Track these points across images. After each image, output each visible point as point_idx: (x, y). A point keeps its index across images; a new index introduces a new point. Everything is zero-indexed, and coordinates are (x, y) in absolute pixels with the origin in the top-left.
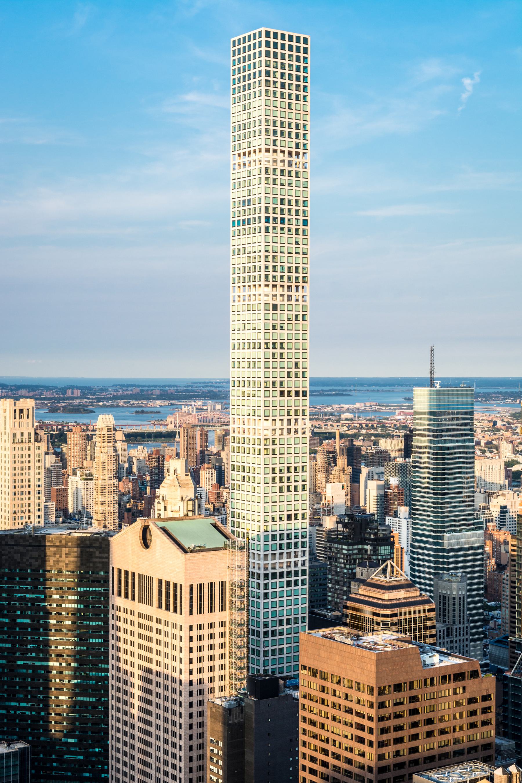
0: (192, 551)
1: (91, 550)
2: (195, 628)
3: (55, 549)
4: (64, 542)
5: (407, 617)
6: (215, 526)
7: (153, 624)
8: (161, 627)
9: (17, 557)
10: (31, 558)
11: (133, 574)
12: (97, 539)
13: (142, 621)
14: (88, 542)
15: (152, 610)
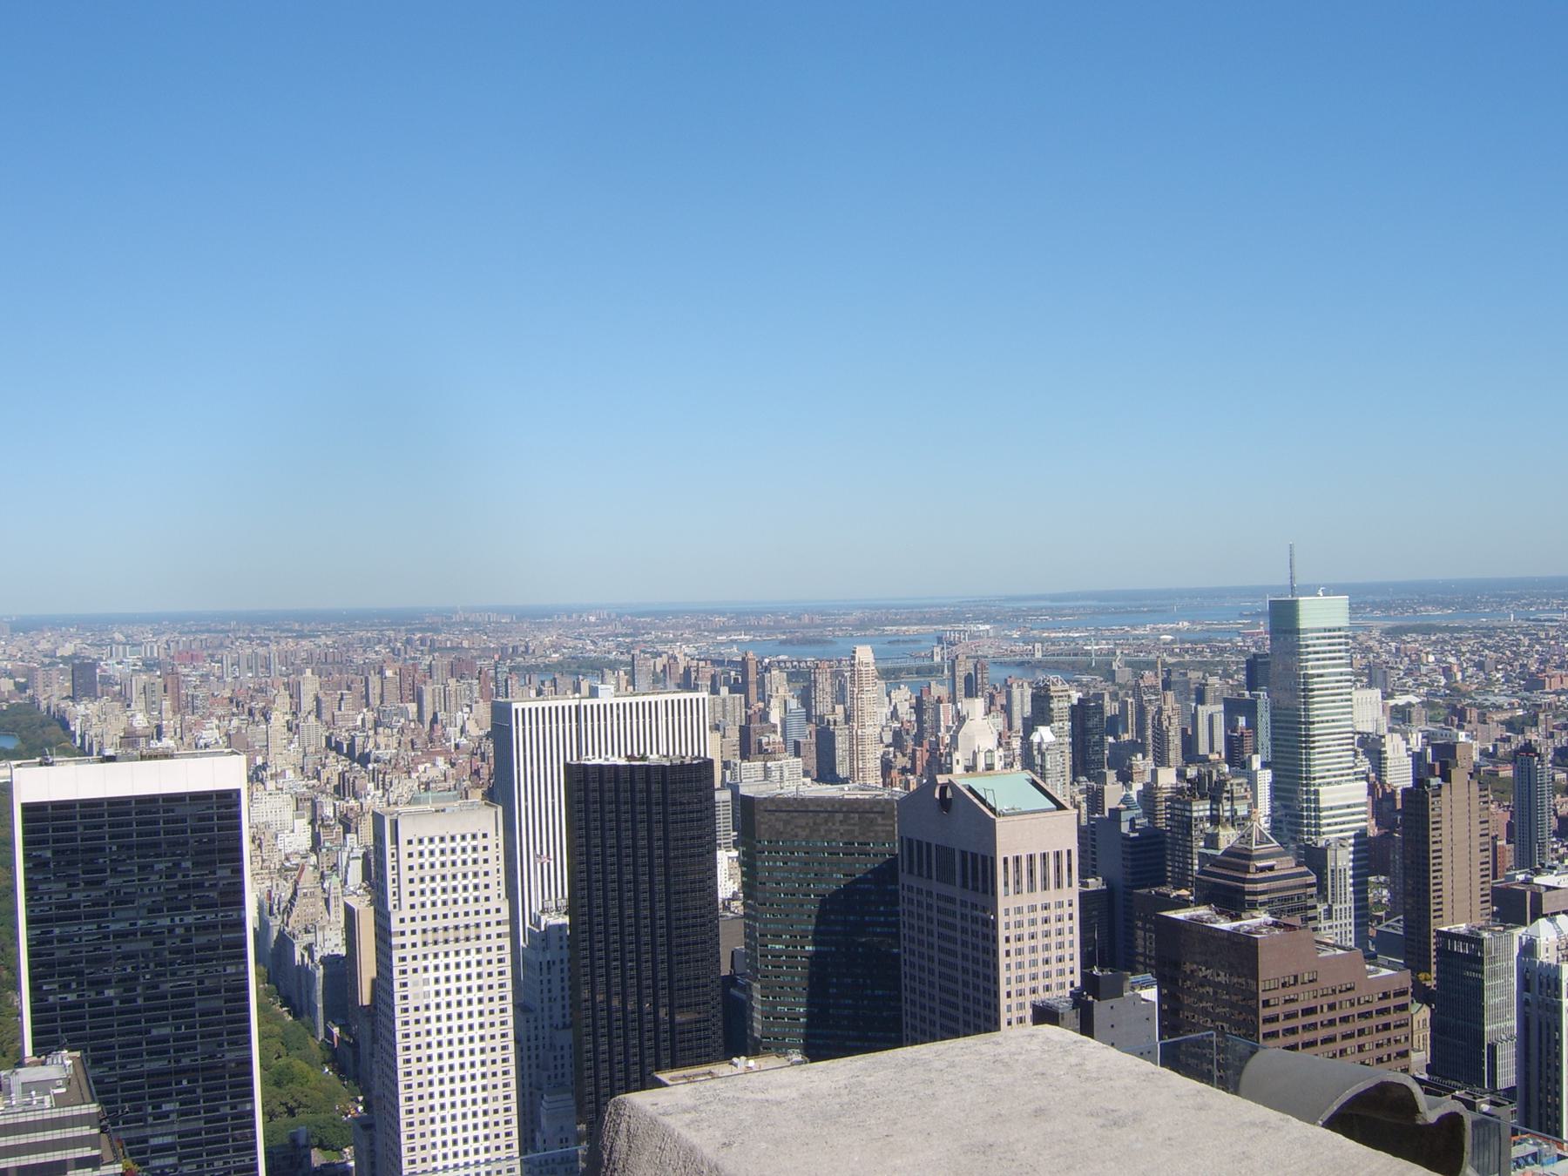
0: (1004, 815)
1: (872, 815)
2: (1012, 912)
3: (826, 815)
4: (837, 806)
5: (1280, 894)
6: (1034, 783)
7: (958, 909)
8: (968, 911)
9: (780, 825)
10: (796, 827)
11: (929, 845)
12: (879, 802)
13: (942, 904)
14: (867, 806)
15: (956, 891)
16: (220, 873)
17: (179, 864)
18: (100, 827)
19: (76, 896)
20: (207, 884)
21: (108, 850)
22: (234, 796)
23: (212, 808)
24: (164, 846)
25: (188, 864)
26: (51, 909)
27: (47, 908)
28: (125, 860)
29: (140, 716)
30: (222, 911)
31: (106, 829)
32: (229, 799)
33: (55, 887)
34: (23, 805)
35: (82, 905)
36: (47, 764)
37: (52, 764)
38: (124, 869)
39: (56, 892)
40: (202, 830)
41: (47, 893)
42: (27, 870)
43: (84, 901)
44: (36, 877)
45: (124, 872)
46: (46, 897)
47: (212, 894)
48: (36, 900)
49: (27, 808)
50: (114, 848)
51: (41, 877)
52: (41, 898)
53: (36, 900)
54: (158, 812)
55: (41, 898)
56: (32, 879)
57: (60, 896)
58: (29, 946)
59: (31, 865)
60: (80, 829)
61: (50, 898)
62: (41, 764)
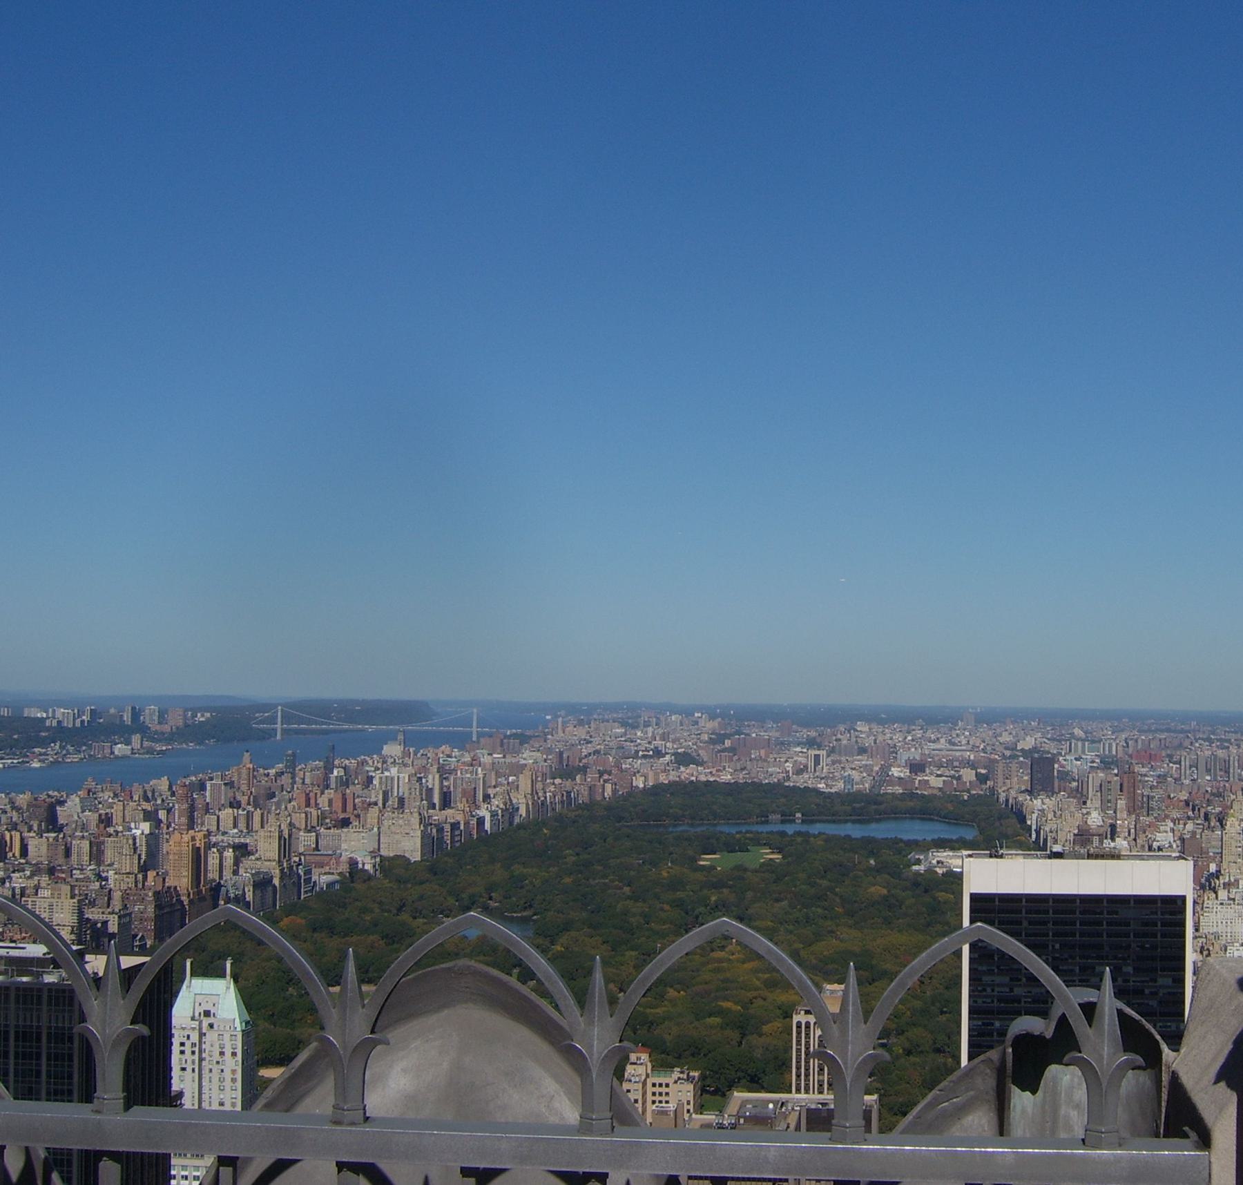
16: (1160, 981)
17: (1121, 968)
18: (1045, 923)
19: (1018, 991)
20: (1147, 991)
21: (1050, 948)
22: (1179, 903)
23: (1156, 913)
24: (1107, 949)
25: (1130, 969)
26: (993, 1002)
27: (989, 1000)
28: (1066, 959)
29: (1095, 814)
30: (1160, 1021)
31: (1050, 925)
32: (1174, 905)
33: (998, 979)
34: (971, 895)
35: (1023, 1000)
36: (996, 857)
37: (1001, 856)
38: (1065, 968)
39: (998, 985)
40: (1145, 935)
41: (989, 985)
42: (971, 960)
43: (1025, 997)
44: (980, 968)
45: (1065, 971)
46: (989, 990)
47: (1151, 1003)
48: (980, 991)
49: (975, 898)
50: (1057, 946)
51: (985, 968)
52: (984, 990)
53: (980, 991)
54: (1101, 913)
55: (984, 990)
56: (976, 969)
57: (1003, 990)
58: (969, 1036)
59: (976, 956)
60: (1025, 924)
61: (993, 991)
62: (991, 856)
